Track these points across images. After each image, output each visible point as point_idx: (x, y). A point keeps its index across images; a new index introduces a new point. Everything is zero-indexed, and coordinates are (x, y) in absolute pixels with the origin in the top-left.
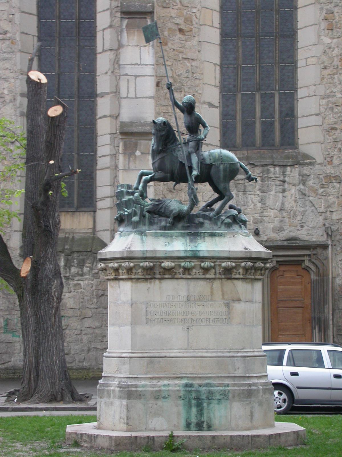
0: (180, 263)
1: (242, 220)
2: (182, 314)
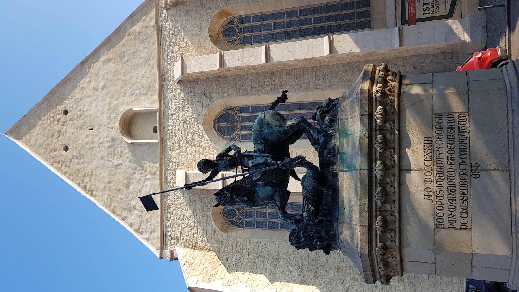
0: (378, 182)
1: (327, 104)
2: (453, 178)
